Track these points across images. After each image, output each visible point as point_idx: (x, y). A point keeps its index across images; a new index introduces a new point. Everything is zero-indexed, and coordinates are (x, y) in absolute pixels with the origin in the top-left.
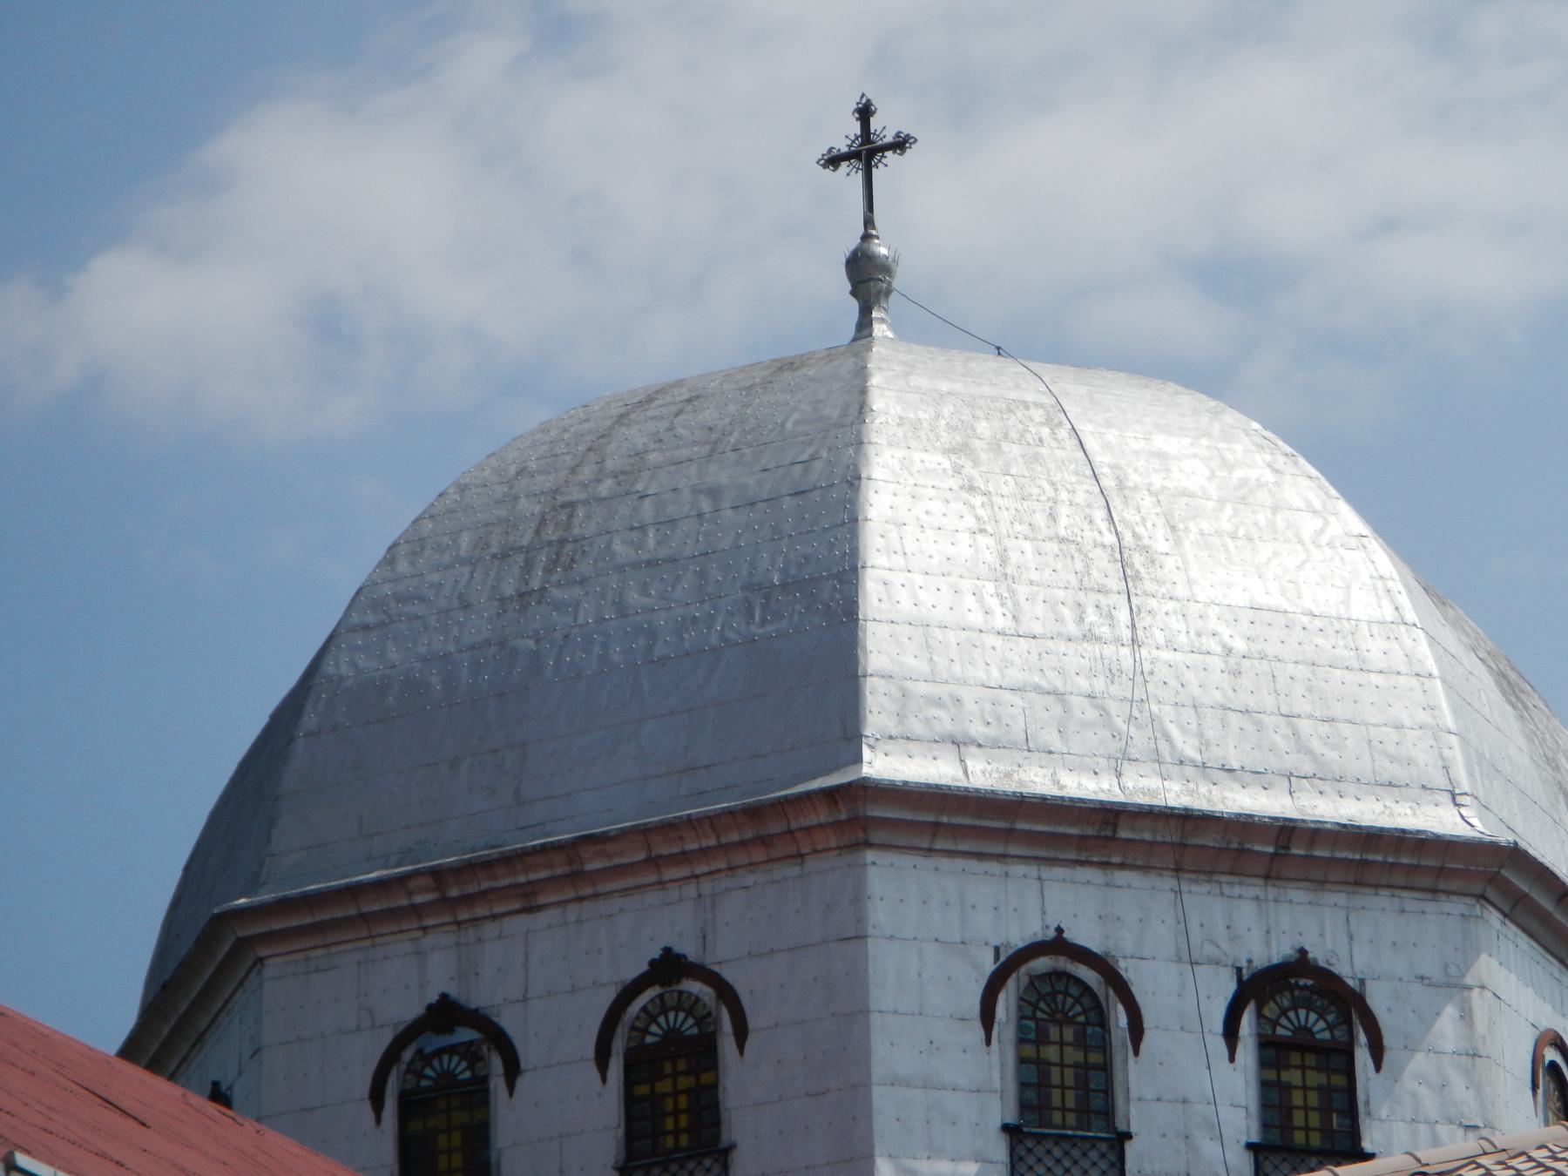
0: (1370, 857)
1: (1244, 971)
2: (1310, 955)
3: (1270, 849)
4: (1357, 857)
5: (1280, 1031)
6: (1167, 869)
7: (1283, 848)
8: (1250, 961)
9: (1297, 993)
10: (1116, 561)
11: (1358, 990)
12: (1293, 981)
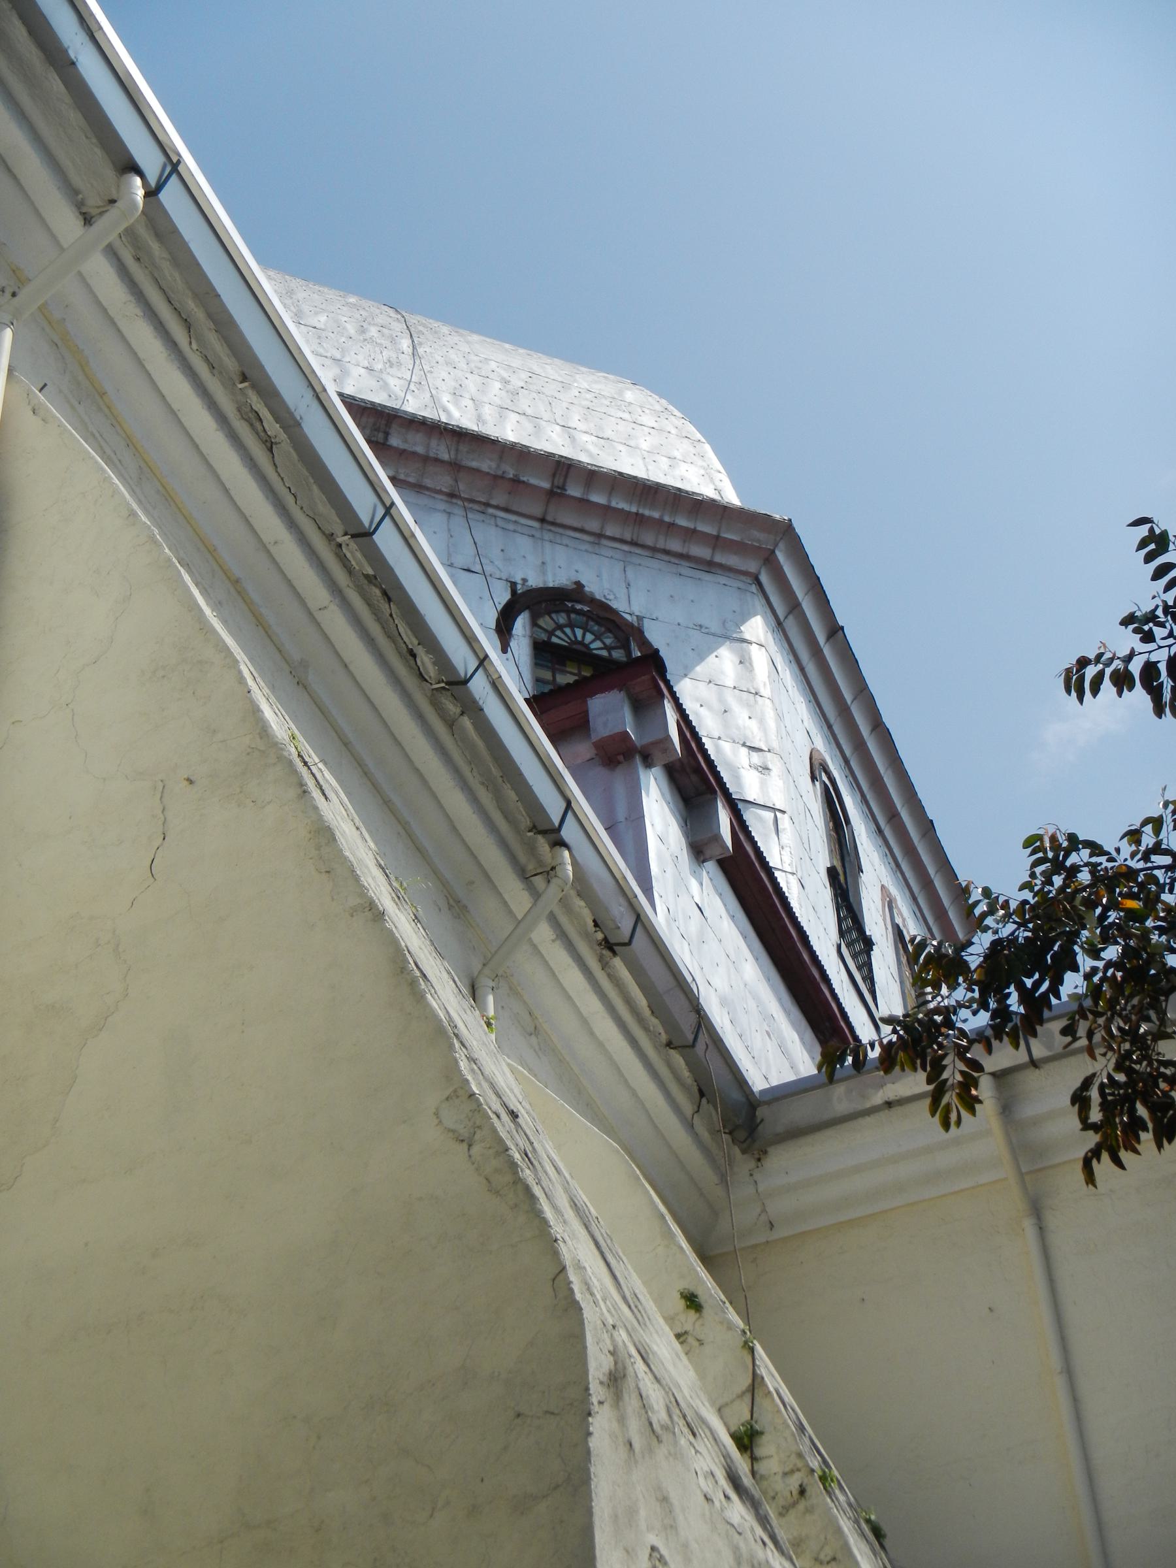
0: (647, 512)
1: (519, 587)
2: (587, 589)
3: (546, 485)
4: (634, 510)
5: (554, 640)
6: (440, 492)
7: (558, 488)
8: (525, 580)
9: (573, 616)
10: (421, 370)
11: (636, 624)
12: (570, 605)
